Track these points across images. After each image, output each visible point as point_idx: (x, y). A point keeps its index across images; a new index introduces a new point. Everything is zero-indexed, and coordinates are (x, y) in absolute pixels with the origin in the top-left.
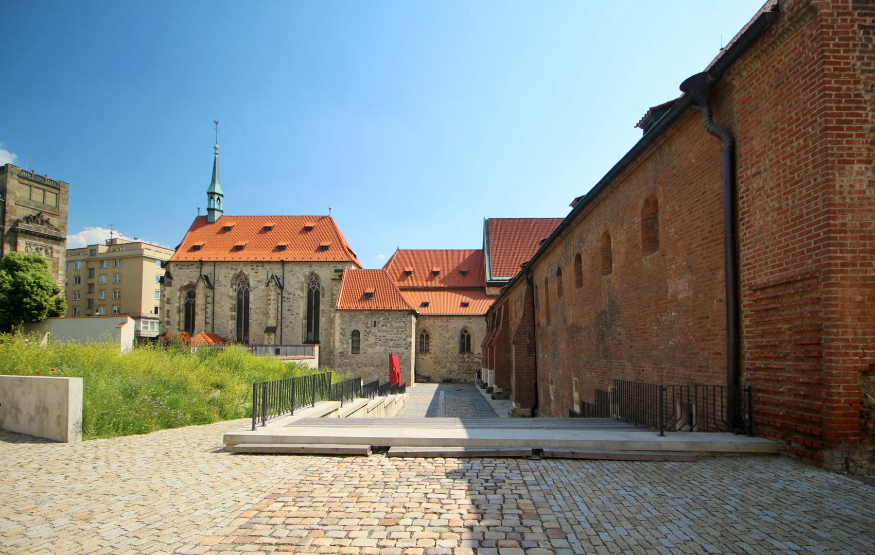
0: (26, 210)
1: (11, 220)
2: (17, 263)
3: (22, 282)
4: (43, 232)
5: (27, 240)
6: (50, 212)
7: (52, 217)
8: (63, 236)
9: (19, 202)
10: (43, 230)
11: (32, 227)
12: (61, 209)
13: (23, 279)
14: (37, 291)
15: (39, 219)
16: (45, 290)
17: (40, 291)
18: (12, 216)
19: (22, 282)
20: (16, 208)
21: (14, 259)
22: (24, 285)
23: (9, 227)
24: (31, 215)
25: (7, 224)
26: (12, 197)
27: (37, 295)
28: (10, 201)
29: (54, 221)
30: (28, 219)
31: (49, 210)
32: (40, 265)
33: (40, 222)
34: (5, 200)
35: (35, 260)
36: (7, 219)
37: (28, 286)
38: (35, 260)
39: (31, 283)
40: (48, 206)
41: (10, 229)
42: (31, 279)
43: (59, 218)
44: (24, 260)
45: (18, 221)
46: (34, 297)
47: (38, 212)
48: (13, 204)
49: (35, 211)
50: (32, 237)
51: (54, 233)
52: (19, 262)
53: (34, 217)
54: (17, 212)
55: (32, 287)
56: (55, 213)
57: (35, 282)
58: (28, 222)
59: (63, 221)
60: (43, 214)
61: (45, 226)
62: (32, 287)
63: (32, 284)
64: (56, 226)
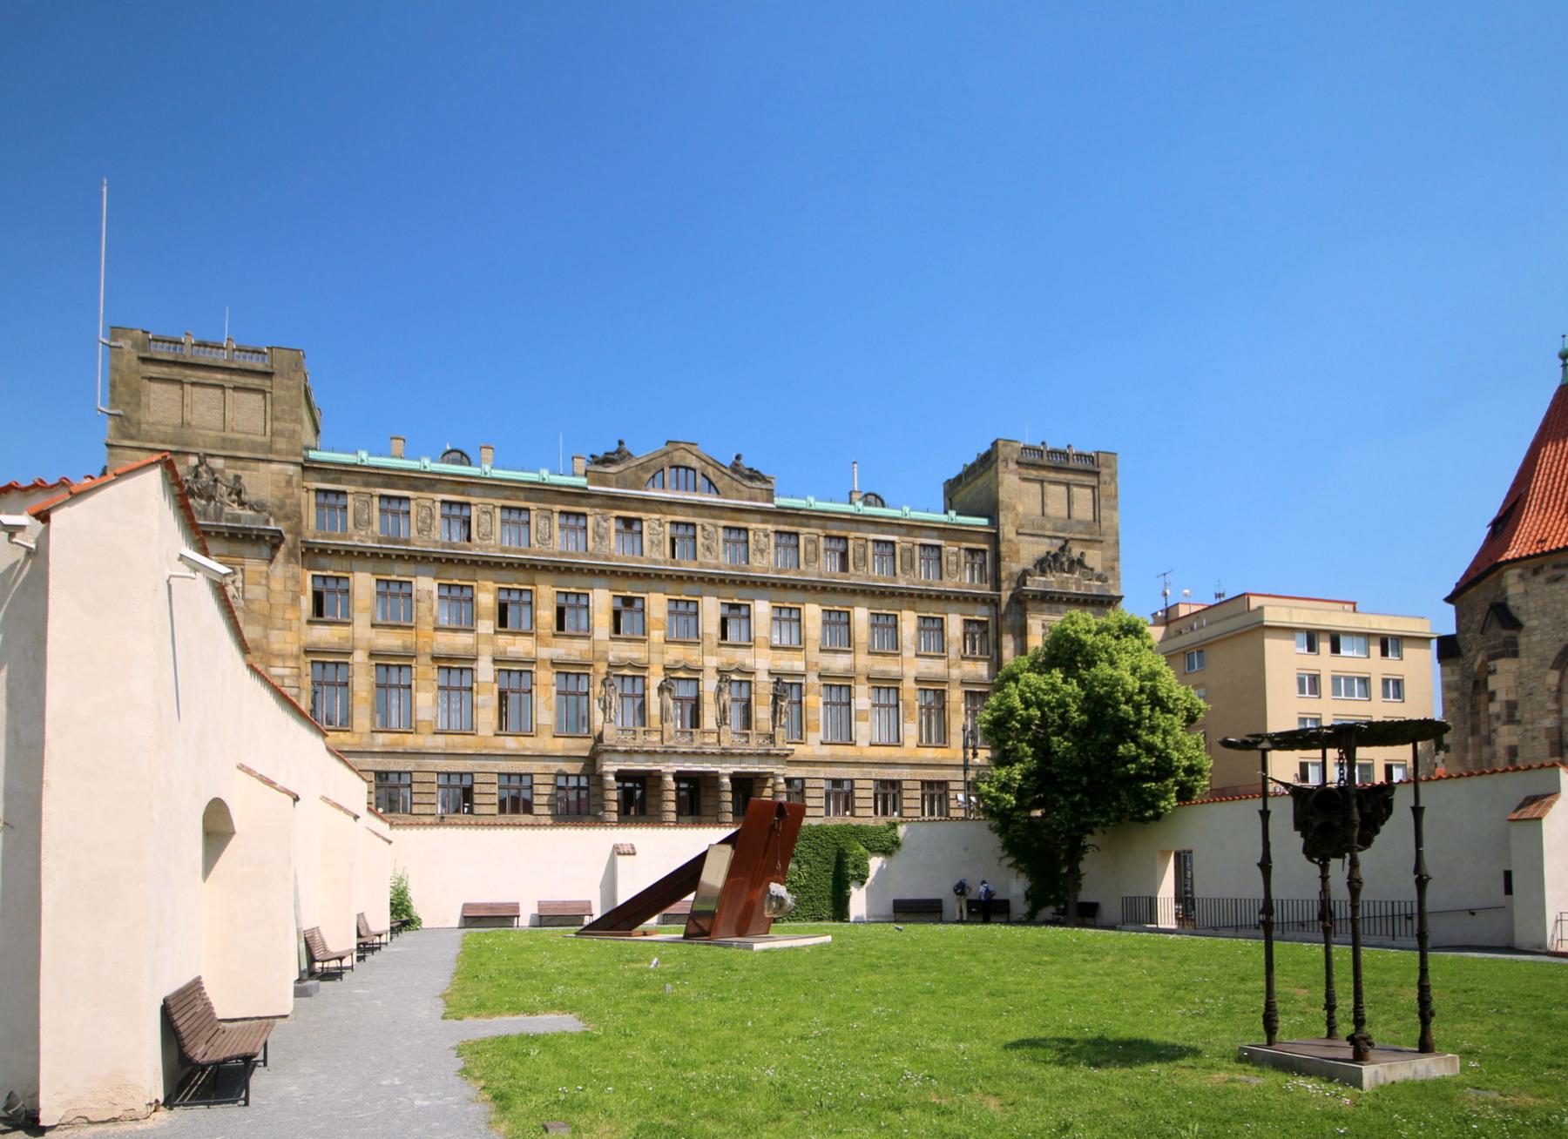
0: (1037, 543)
1: (1011, 574)
2: (1082, 645)
3: (1110, 695)
4: (1073, 590)
5: (1045, 617)
6: (1084, 537)
7: (1088, 548)
8: (1114, 593)
9: (1022, 526)
10: (1073, 583)
11: (1051, 581)
12: (1104, 523)
13: (1115, 682)
14: (1150, 718)
15: (1064, 559)
16: (1170, 711)
17: (1161, 719)
18: (1013, 565)
19: (1110, 695)
20: (1019, 542)
21: (1076, 632)
22: (1119, 703)
23: (1009, 593)
24: (1048, 553)
25: (1005, 586)
26: (1011, 516)
27: (1152, 730)
28: (1006, 529)
29: (1094, 558)
30: (1043, 565)
31: (1081, 533)
32: (1137, 643)
33: (1066, 566)
34: (998, 529)
35: (1121, 628)
36: (1004, 575)
37: (1126, 703)
38: (1121, 628)
39: (1132, 695)
40: (1079, 522)
41: (1012, 596)
42: (1132, 683)
43: (1102, 550)
44: (1097, 633)
45: (1025, 573)
46: (1146, 737)
47: (1060, 543)
48: (1012, 536)
49: (1055, 541)
50: (1054, 607)
51: (1095, 587)
52: (1089, 639)
53: (1055, 556)
54: (1021, 552)
55: (1138, 708)
56: (1094, 537)
57: (1142, 691)
58: (1043, 573)
59: (1110, 554)
60: (1069, 545)
61: (1076, 575)
62: (1138, 708)
63: (1136, 698)
64: (1098, 570)
